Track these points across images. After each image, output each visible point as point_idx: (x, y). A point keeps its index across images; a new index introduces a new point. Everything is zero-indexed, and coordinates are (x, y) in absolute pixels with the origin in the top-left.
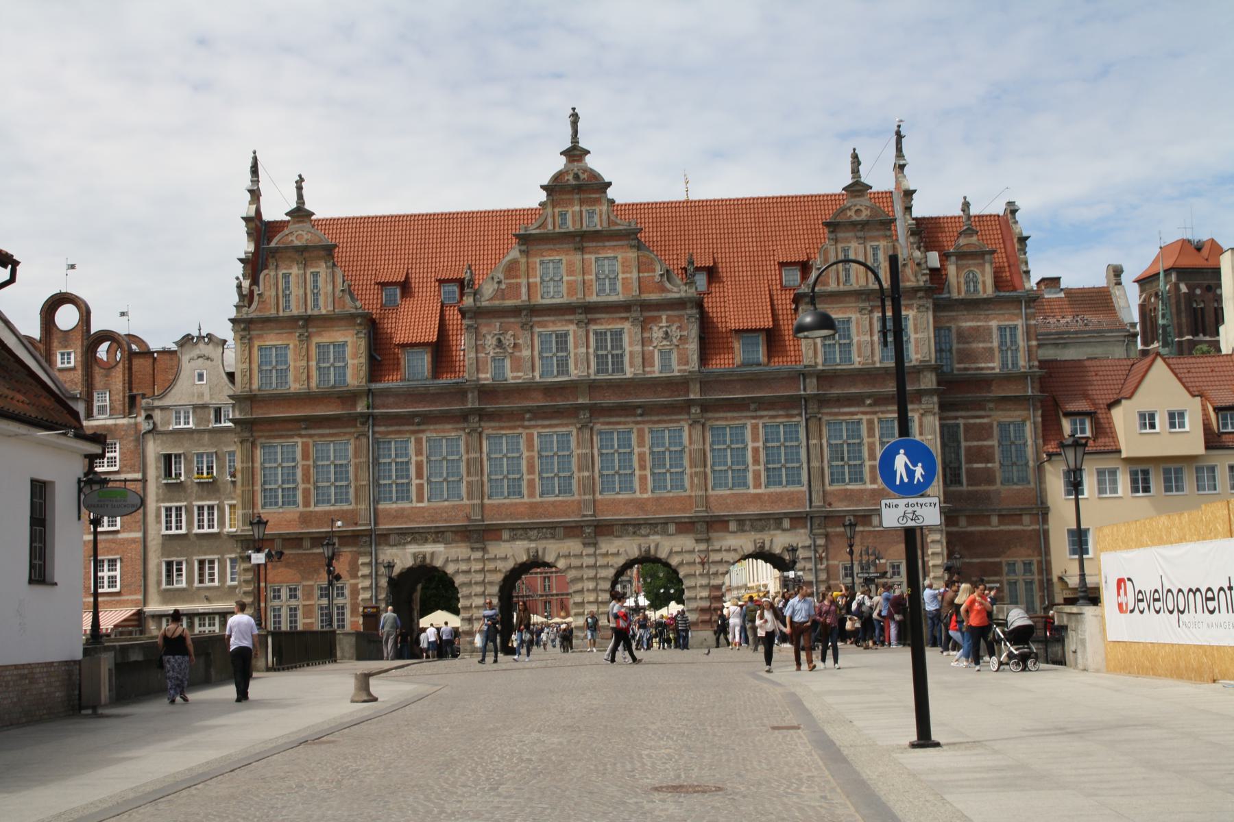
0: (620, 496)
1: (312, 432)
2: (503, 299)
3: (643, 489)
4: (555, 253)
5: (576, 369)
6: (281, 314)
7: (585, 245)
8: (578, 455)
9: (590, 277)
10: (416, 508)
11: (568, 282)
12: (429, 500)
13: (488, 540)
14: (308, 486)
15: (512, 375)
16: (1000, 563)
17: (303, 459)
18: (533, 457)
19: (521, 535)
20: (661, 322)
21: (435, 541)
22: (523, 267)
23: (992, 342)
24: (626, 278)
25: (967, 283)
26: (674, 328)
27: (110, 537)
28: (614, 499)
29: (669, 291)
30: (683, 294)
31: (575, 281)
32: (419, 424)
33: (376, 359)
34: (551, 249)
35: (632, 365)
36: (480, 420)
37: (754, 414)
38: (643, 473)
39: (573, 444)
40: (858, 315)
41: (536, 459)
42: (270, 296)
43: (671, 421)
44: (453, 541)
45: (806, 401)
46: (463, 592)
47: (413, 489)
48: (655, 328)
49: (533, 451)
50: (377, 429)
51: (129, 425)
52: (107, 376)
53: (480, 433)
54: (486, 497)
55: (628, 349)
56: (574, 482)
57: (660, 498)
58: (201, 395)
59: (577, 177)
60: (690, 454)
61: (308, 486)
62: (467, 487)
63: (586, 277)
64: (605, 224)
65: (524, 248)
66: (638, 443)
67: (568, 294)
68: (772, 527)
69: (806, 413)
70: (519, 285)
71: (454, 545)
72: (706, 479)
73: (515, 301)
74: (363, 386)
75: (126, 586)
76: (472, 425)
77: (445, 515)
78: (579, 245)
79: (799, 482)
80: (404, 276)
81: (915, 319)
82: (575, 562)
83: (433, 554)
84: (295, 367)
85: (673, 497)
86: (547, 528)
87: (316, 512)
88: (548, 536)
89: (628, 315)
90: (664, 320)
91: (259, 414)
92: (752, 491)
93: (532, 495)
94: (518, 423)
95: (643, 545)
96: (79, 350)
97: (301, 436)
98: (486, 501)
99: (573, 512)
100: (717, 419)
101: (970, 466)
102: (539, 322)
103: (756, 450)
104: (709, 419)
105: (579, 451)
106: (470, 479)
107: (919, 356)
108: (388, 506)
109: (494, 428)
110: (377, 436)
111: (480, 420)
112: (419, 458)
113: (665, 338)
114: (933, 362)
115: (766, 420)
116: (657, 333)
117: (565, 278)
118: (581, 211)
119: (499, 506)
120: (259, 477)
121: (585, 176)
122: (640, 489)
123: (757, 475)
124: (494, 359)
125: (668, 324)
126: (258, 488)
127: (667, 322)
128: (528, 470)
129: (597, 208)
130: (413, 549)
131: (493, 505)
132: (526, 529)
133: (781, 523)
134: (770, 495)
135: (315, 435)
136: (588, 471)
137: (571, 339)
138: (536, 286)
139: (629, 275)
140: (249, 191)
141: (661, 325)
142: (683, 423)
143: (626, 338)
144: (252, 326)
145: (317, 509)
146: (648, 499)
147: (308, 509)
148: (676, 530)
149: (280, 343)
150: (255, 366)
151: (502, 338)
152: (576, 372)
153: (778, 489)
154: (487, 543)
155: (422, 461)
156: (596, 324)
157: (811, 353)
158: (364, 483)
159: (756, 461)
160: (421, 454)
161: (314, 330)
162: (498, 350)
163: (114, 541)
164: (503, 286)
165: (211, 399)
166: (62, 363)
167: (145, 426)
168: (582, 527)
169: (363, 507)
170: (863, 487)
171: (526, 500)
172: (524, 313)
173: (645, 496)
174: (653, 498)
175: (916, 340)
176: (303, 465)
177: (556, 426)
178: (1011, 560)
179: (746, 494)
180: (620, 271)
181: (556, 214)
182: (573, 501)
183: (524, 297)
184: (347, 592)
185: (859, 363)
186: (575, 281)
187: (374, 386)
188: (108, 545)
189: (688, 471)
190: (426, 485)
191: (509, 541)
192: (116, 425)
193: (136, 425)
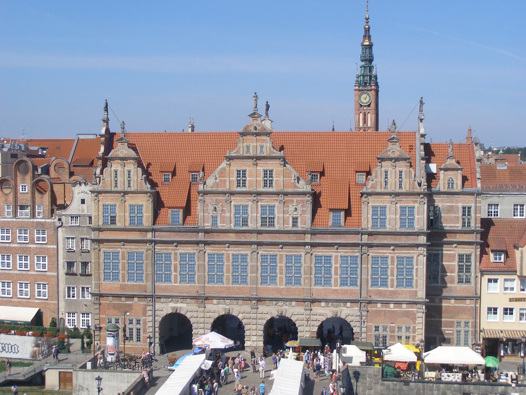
1: (127, 247)
2: (218, 187)
3: (281, 284)
6: (113, 189)
8: (251, 265)
9: (260, 179)
14: (124, 272)
15: (220, 225)
16: (454, 321)
17: (122, 260)
18: (229, 265)
21: (181, 302)
22: (227, 172)
23: (458, 214)
25: (449, 183)
26: (300, 206)
27: (43, 273)
29: (298, 188)
30: (305, 190)
32: (176, 246)
34: (241, 164)
38: (281, 276)
39: (249, 260)
40: (390, 205)
41: (231, 266)
42: (108, 181)
43: (296, 252)
46: (194, 326)
47: (173, 277)
48: (290, 206)
49: (229, 262)
51: (52, 222)
52: (41, 198)
53: (205, 252)
55: (277, 215)
56: (248, 278)
58: (83, 210)
59: (256, 128)
61: (124, 272)
63: (257, 179)
64: (268, 153)
65: (228, 163)
66: (280, 261)
67: (249, 186)
70: (225, 181)
73: (223, 189)
74: (150, 227)
75: (51, 297)
76: (200, 248)
77: (187, 290)
78: (255, 163)
79: (356, 285)
80: (173, 168)
81: (418, 208)
82: (247, 315)
83: (181, 308)
84: (119, 215)
87: (128, 285)
88: (235, 303)
89: (278, 198)
90: (295, 202)
91: (103, 236)
92: (333, 288)
93: (228, 283)
95: (279, 311)
96: (29, 185)
97: (121, 248)
98: (206, 285)
100: (318, 252)
101: (442, 274)
103: (336, 268)
104: (314, 252)
105: (251, 264)
106: (199, 274)
107: (419, 227)
108: (161, 284)
109: (211, 250)
112: (176, 262)
114: (425, 230)
116: (291, 208)
119: (212, 287)
120: (102, 266)
121: (259, 128)
123: (336, 280)
126: (102, 271)
128: (226, 271)
129: (265, 145)
130: (172, 305)
131: (209, 287)
134: (342, 290)
135: (128, 248)
136: (255, 273)
137: (249, 209)
139: (279, 179)
140: (104, 121)
141: (293, 204)
142: (301, 253)
143: (276, 210)
144: (99, 195)
145: (128, 283)
146: (283, 288)
147: (124, 283)
149: (112, 203)
150: (101, 214)
152: (251, 225)
153: (346, 288)
155: (177, 264)
156: (262, 202)
157: (366, 222)
158: (150, 273)
159: (336, 274)
160: (177, 261)
161: (128, 198)
162: (214, 212)
163: (45, 276)
164: (218, 181)
165: (88, 212)
166: (22, 190)
167: (58, 224)
169: (149, 284)
170: (387, 289)
171: (225, 285)
172: (228, 195)
173: (282, 287)
175: (418, 218)
176: (122, 262)
178: (459, 320)
179: (330, 289)
181: (245, 146)
182: (247, 287)
183: (228, 187)
184: (141, 322)
185: (389, 228)
186: (252, 180)
187: (155, 227)
188: (42, 277)
189: (303, 276)
192: (45, 222)
193: (54, 222)
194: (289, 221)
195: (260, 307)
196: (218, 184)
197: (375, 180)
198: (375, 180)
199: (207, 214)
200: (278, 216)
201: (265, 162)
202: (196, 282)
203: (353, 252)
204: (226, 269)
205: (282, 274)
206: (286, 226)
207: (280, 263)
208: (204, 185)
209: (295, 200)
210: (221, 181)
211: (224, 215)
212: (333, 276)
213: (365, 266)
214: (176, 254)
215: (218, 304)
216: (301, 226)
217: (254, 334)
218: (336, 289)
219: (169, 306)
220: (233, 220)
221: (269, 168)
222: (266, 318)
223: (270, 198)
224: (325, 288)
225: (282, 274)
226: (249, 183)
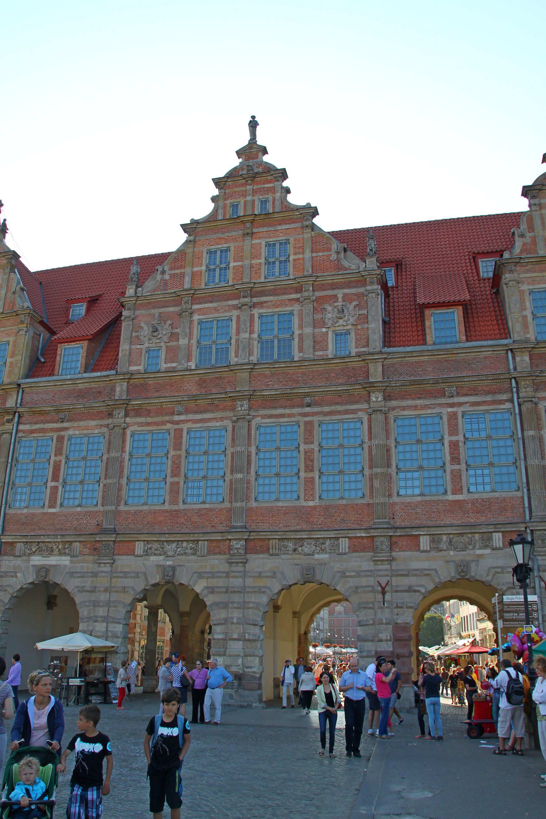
0: (280, 504)
4: (223, 241)
5: (236, 357)
7: (255, 230)
8: (232, 454)
9: (259, 261)
10: (48, 513)
11: (234, 267)
12: (61, 505)
13: (118, 555)
15: (165, 366)
18: (180, 457)
19: (156, 550)
20: (337, 301)
21: (60, 554)
22: (189, 257)
24: (299, 259)
26: (351, 307)
28: (272, 508)
29: (346, 269)
31: (242, 266)
33: (40, 361)
35: (301, 350)
36: (126, 415)
37: (451, 401)
38: (310, 475)
43: (346, 412)
44: (81, 553)
45: (517, 383)
48: (329, 308)
50: (21, 427)
54: (123, 502)
55: (297, 332)
57: (330, 506)
60: (370, 451)
62: (104, 491)
67: (234, 279)
68: (477, 546)
69: (518, 398)
70: (183, 274)
71: (80, 558)
72: (390, 482)
85: (346, 505)
86: (187, 541)
88: (189, 551)
89: (298, 296)
90: (340, 299)
93: (174, 501)
94: (167, 418)
99: (221, 523)
100: (404, 408)
102: (200, 309)
103: (454, 446)
104: (394, 409)
106: (109, 481)
108: (19, 512)
109: (139, 424)
110: (20, 435)
111: (126, 415)
112: (58, 458)
113: (341, 318)
115: (466, 408)
116: (330, 313)
117: (232, 264)
118: (254, 201)
119: (135, 512)
122: (305, 495)
124: (148, 351)
125: (344, 304)
127: (343, 301)
129: (270, 197)
130: (37, 560)
131: (128, 513)
132: (163, 541)
133: (490, 539)
134: (474, 502)
136: (241, 471)
138: (201, 274)
142: (361, 414)
146: (315, 507)
148: (349, 548)
151: (159, 328)
152: (236, 359)
154: (116, 557)
155: (60, 461)
156: (262, 307)
160: (61, 454)
162: (154, 340)
164: (167, 277)
168: (230, 540)
171: (167, 507)
173: (311, 504)
174: (321, 506)
177: (210, 420)
179: (442, 501)
180: (292, 252)
181: (228, 206)
182: (221, 510)
189: (367, 472)
190: (60, 488)
191: (141, 556)
194: (327, 341)
195: (251, 557)
196: (166, 284)
197: (528, 235)
198: (528, 235)
199: (139, 347)
200: (300, 335)
201: (270, 229)
202: (100, 502)
203: (494, 402)
204: (172, 466)
205: (312, 471)
206: (320, 353)
207: (306, 443)
208: (137, 287)
209: (340, 296)
210: (172, 276)
211: (175, 343)
212: (448, 465)
213: (531, 433)
214: (60, 439)
215: (147, 553)
216: (356, 350)
217: (235, 636)
218: (459, 501)
219: (32, 563)
220: (194, 353)
221: (280, 238)
222: (269, 588)
223: (280, 298)
224: (428, 498)
225: (312, 471)
226: (234, 273)
